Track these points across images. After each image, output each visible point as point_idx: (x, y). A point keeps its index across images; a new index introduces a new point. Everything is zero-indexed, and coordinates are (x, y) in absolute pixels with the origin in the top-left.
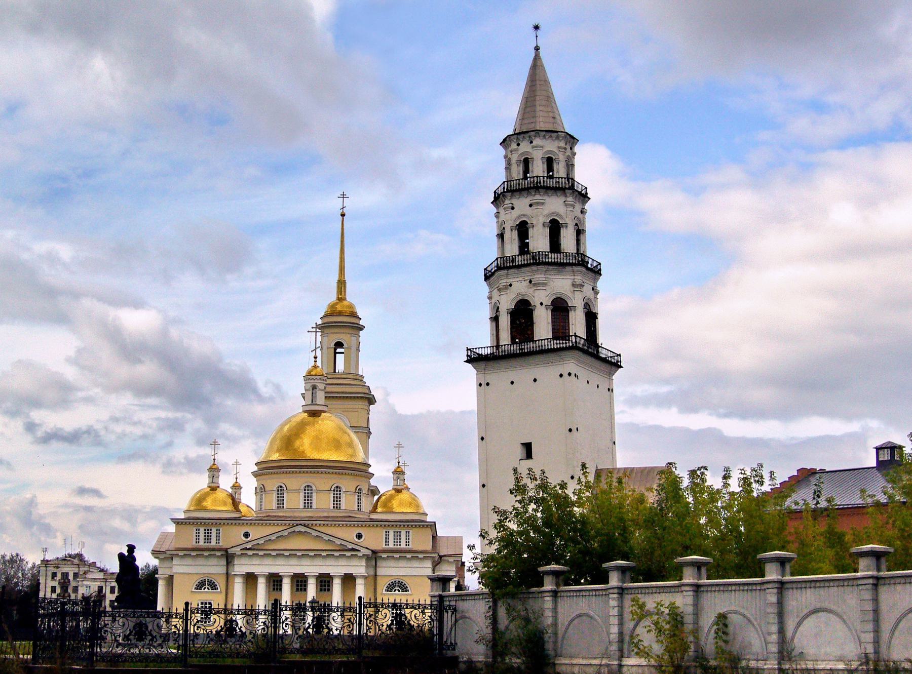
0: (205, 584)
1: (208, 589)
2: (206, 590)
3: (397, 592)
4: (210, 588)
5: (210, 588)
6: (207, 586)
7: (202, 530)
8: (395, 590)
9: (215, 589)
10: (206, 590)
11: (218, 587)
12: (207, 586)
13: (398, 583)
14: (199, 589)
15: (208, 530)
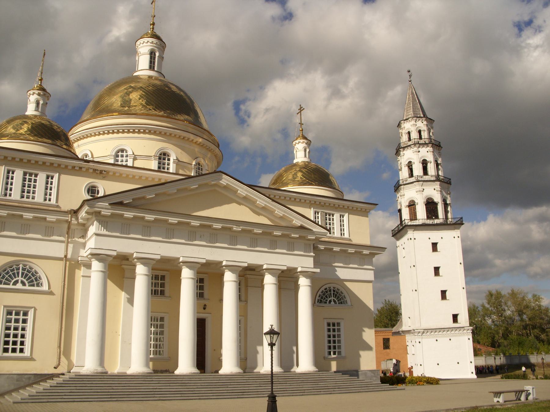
0: (18, 273)
1: (23, 284)
2: (19, 286)
3: (332, 303)
4: (26, 282)
5: (26, 282)
6: (20, 278)
7: (18, 174)
8: (330, 302)
9: (38, 285)
10: (19, 286)
11: (44, 281)
12: (20, 278)
13: (334, 291)
14: (5, 284)
15: (31, 175)
